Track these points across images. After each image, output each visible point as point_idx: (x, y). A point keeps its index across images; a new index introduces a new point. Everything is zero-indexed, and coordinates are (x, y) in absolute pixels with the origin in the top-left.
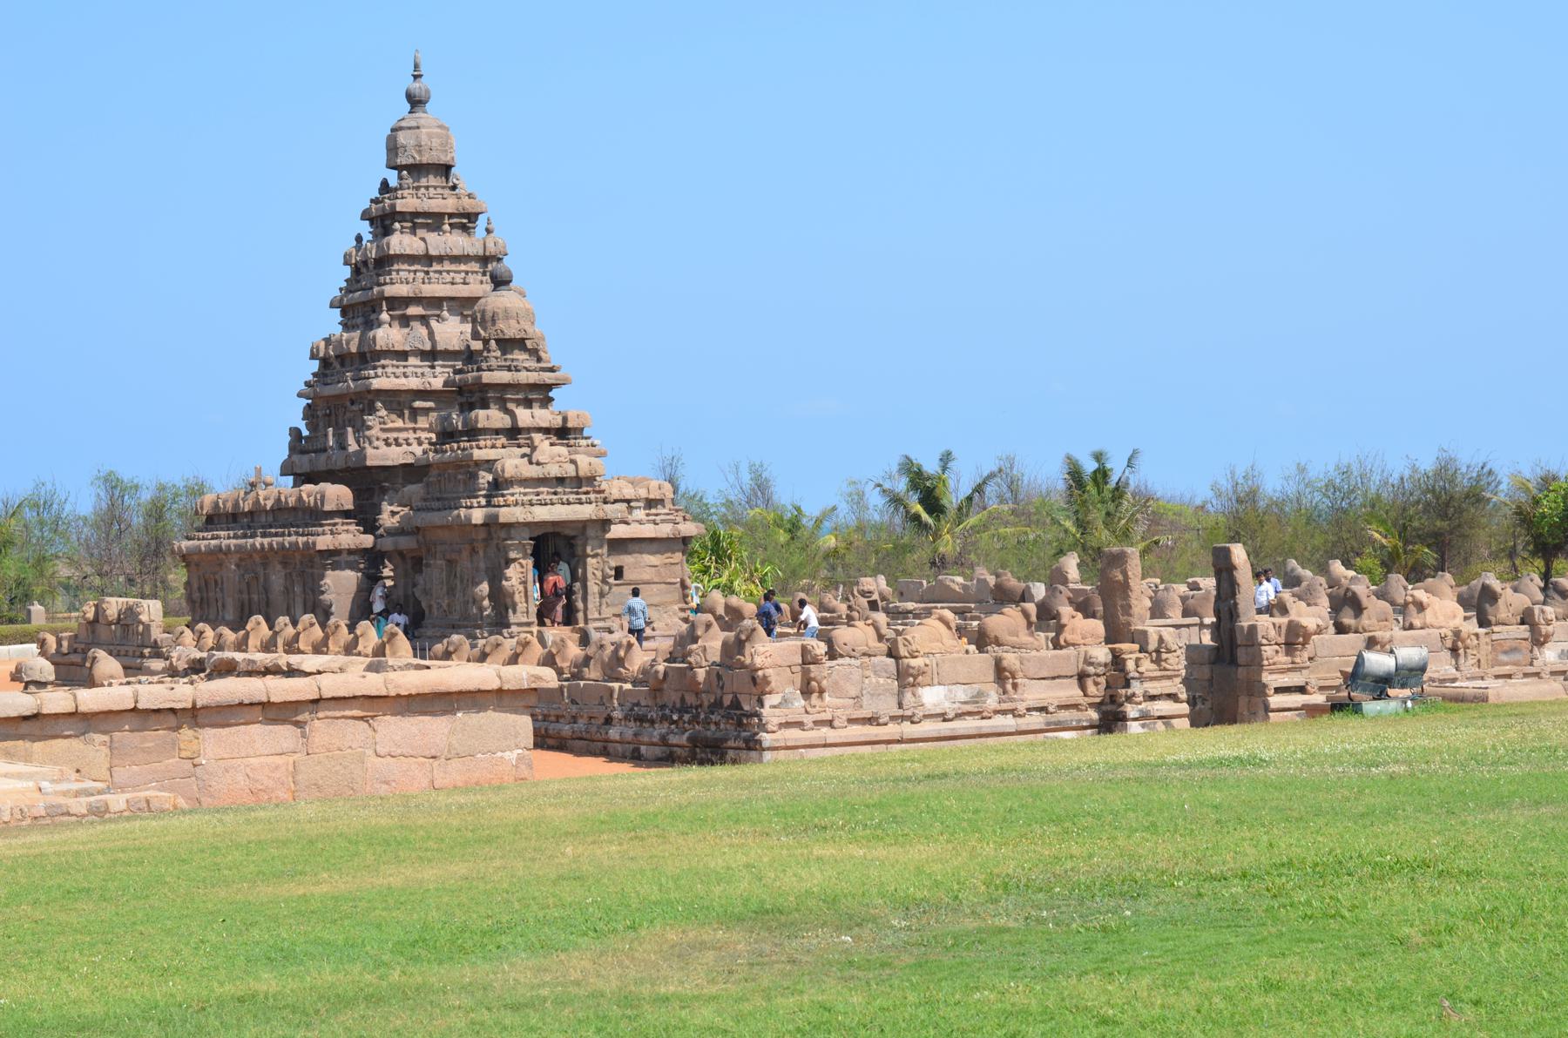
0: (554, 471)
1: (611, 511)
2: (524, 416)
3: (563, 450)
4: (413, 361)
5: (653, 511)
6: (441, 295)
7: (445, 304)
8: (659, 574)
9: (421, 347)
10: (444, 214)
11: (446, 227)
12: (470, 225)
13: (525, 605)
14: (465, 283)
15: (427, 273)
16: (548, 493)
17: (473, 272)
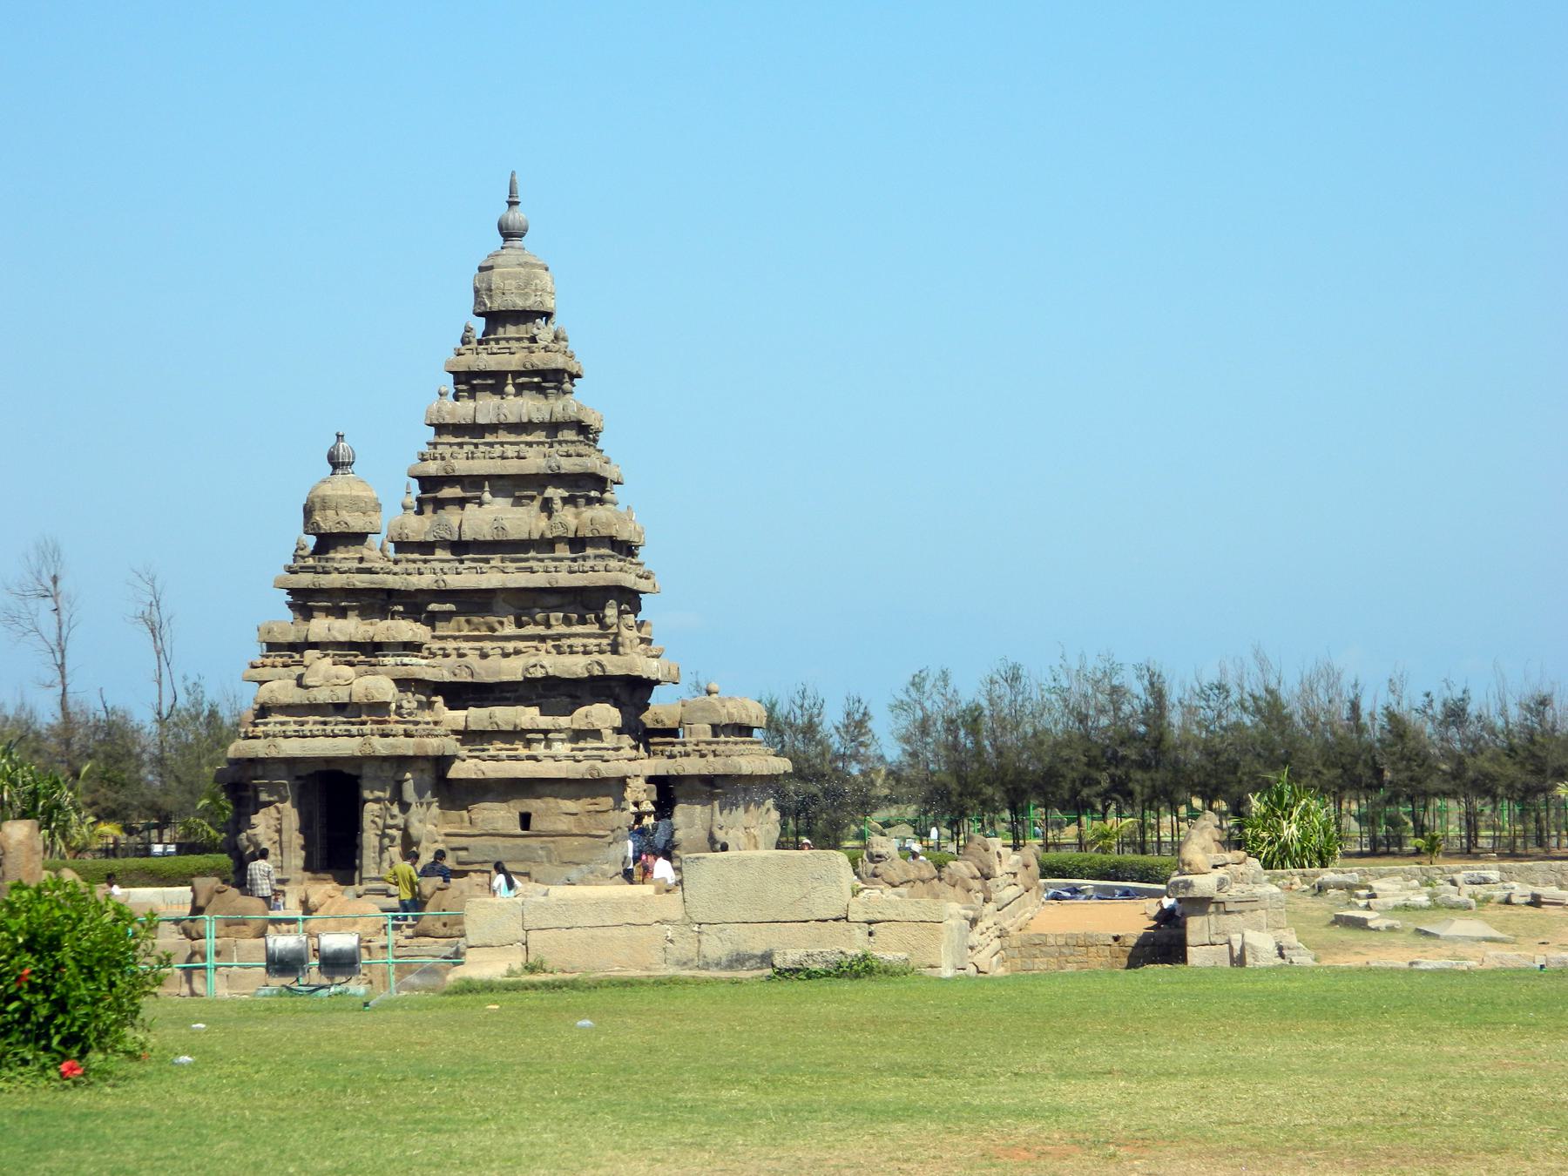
0: (322, 696)
1: (381, 746)
2: (321, 627)
3: (348, 671)
4: (440, 554)
5: (581, 744)
7: (487, 483)
8: (580, 824)
9: (448, 537)
10: (505, 373)
11: (510, 389)
13: (280, 858)
14: (519, 457)
15: (476, 446)
16: (315, 723)
17: (538, 443)
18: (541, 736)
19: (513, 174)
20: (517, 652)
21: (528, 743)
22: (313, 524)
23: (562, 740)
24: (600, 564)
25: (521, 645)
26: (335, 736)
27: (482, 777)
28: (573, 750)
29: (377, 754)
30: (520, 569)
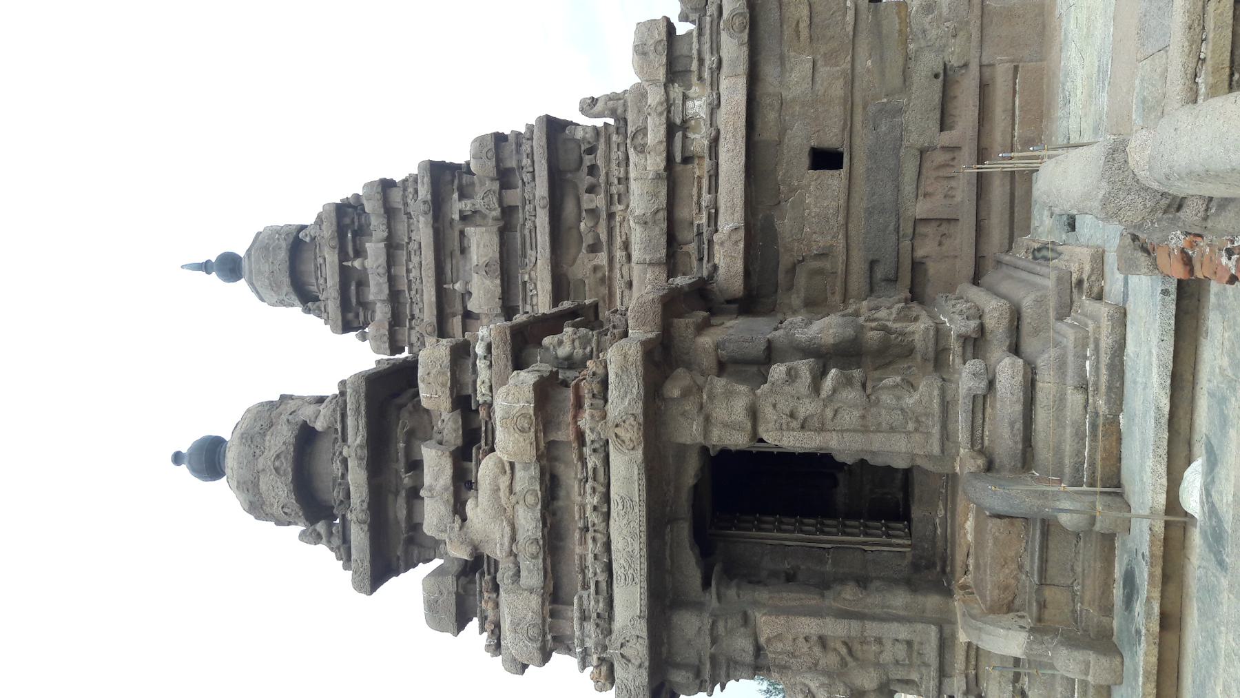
0: (528, 522)
6: (433, 292)
7: (445, 286)
8: (830, 58)
11: (357, 264)
12: (356, 224)
16: (583, 542)
18: (679, 136)
19: (182, 267)
20: (626, 246)
21: (687, 160)
22: (284, 512)
23: (685, 98)
24: (526, 147)
25: (618, 241)
26: (607, 498)
27: (742, 233)
28: (700, 78)
29: (638, 409)
30: (534, 247)
